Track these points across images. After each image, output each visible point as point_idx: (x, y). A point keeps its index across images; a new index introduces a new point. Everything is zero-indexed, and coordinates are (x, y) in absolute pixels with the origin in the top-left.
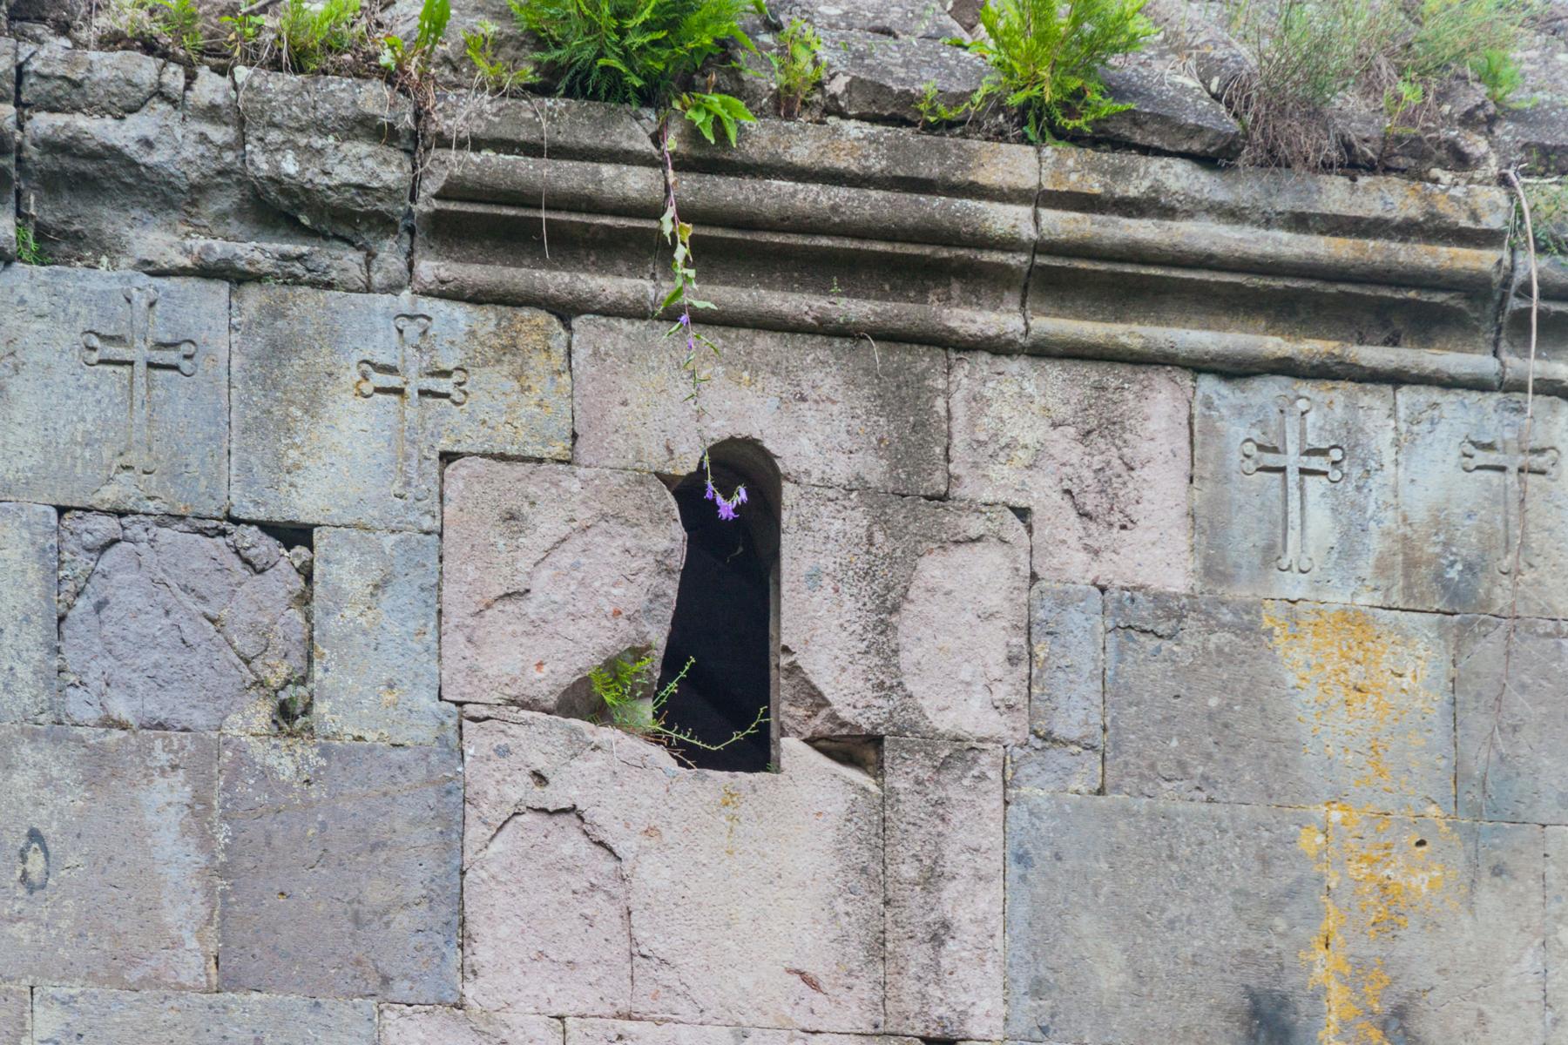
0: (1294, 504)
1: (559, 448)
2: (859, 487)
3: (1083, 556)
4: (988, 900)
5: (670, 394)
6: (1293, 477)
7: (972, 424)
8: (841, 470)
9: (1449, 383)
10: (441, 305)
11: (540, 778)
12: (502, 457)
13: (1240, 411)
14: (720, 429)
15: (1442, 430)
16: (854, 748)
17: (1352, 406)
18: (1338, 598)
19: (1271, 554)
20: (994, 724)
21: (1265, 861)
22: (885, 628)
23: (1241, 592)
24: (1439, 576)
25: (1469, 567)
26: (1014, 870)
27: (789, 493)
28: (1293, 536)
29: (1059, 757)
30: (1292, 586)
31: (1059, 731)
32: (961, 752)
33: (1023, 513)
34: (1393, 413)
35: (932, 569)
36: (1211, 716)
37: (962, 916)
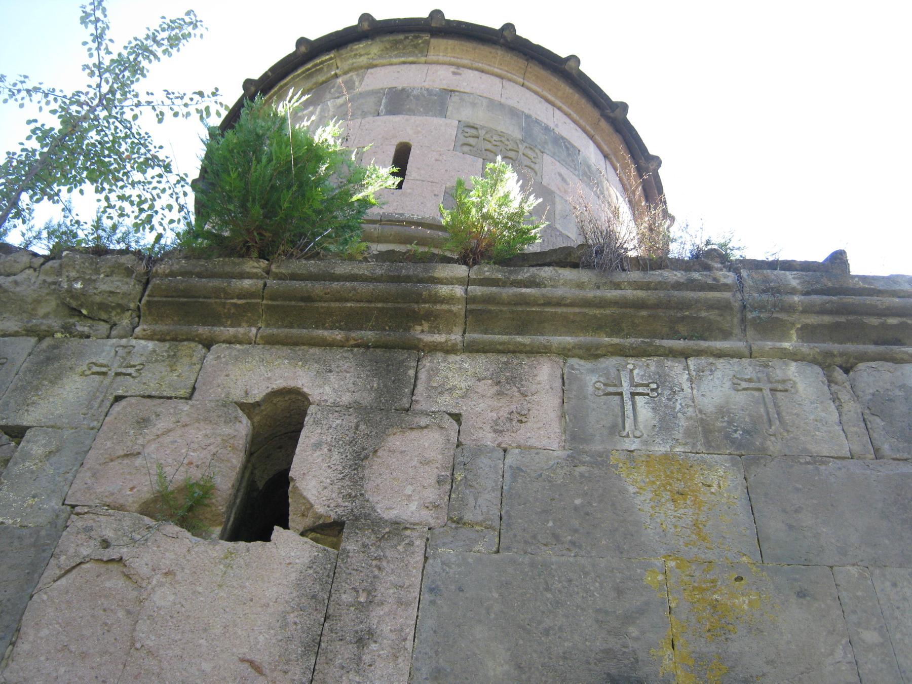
0: (628, 407)
1: (182, 393)
2: (356, 407)
3: (493, 435)
4: (407, 618)
5: (254, 373)
6: (627, 397)
7: (429, 379)
8: (346, 398)
9: (720, 355)
10: (143, 342)
11: (106, 544)
12: (150, 397)
13: (592, 371)
14: (279, 384)
15: (718, 374)
16: (328, 531)
17: (660, 365)
18: (660, 449)
19: (616, 429)
20: (427, 516)
21: (620, 592)
22: (356, 467)
23: (597, 447)
24: (727, 436)
25: (746, 432)
26: (426, 597)
27: (312, 409)
28: (629, 423)
29: (464, 532)
30: (632, 444)
31: (468, 516)
32: (398, 528)
33: (457, 417)
34: (687, 367)
35: (395, 441)
36: (576, 509)
37: (386, 628)
